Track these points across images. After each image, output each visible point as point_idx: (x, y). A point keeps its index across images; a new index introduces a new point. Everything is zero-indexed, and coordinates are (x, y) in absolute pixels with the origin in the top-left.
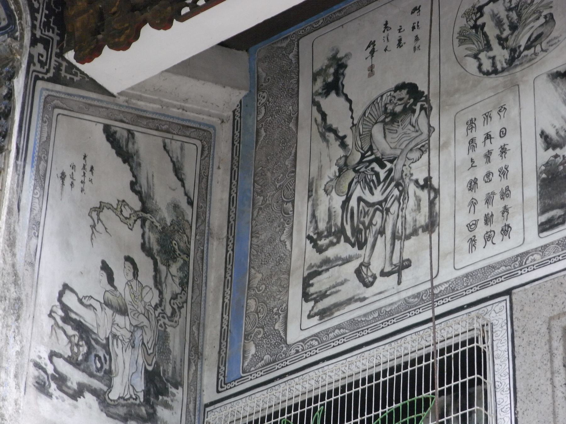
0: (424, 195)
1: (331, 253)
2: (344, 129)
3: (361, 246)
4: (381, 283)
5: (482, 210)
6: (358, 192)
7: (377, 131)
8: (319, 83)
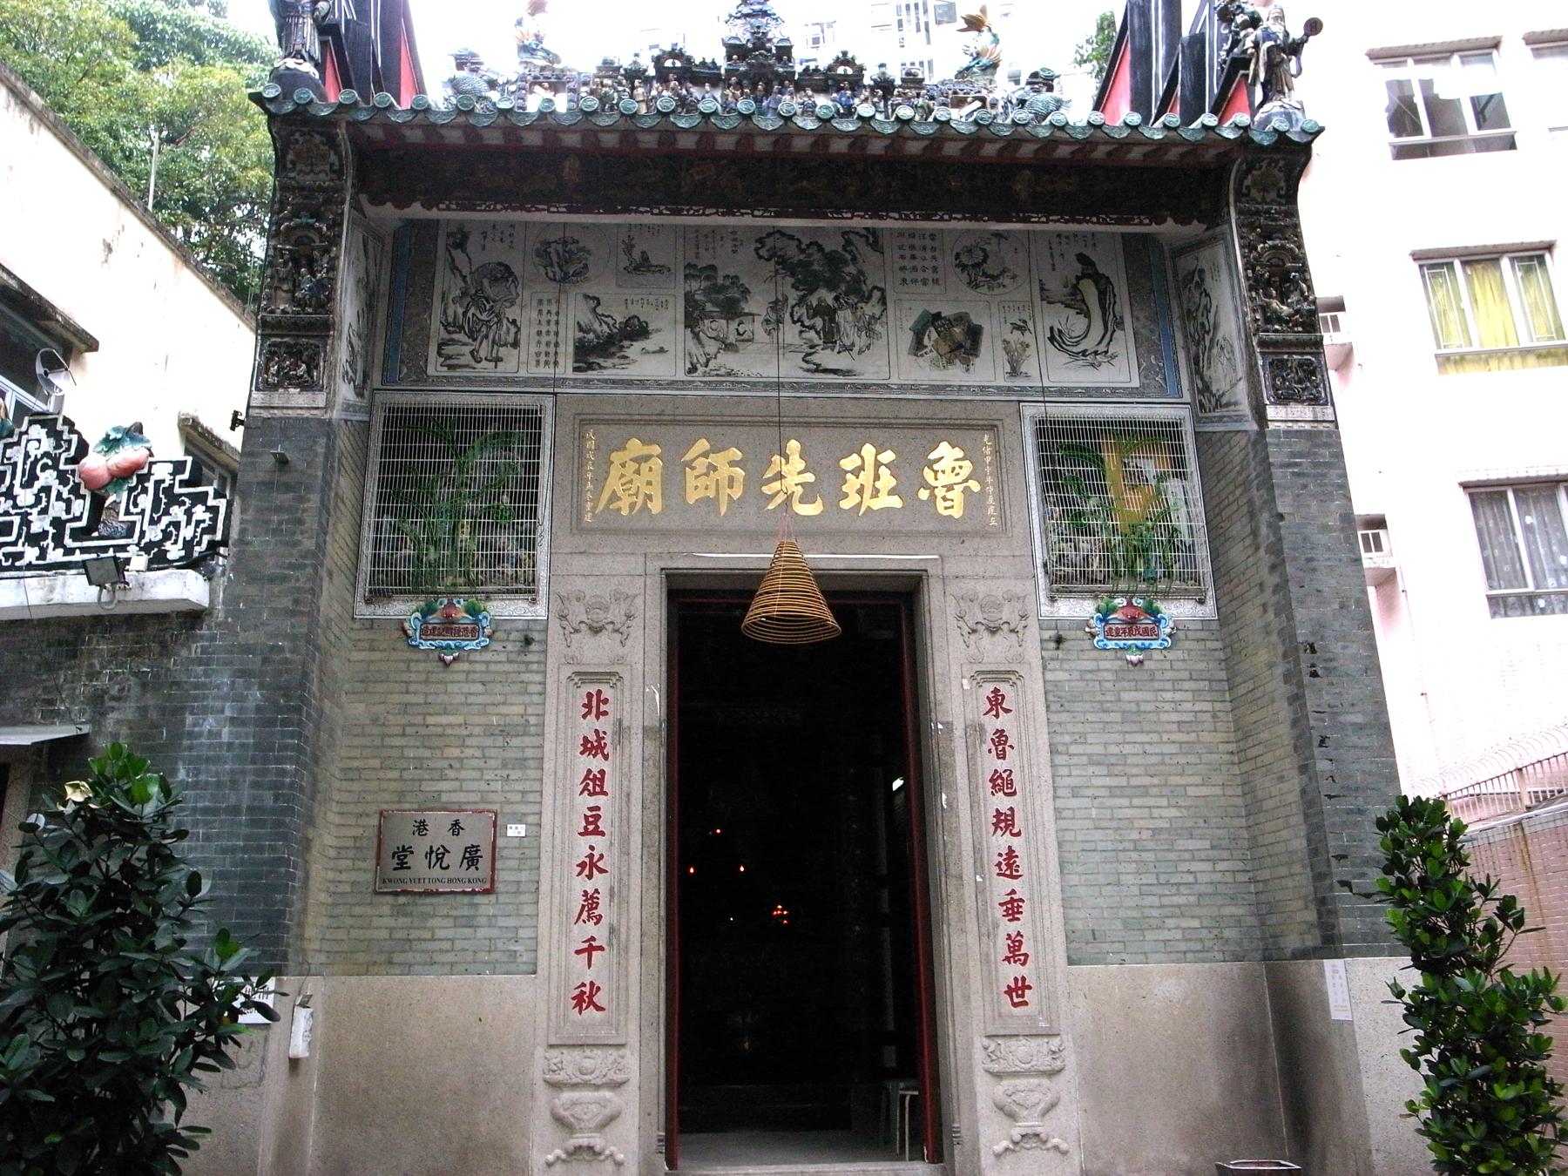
0: (513, 330)
1: (455, 336)
2: (466, 272)
3: (474, 340)
4: (484, 364)
5: (543, 348)
6: (472, 310)
7: (486, 282)
8: (451, 240)
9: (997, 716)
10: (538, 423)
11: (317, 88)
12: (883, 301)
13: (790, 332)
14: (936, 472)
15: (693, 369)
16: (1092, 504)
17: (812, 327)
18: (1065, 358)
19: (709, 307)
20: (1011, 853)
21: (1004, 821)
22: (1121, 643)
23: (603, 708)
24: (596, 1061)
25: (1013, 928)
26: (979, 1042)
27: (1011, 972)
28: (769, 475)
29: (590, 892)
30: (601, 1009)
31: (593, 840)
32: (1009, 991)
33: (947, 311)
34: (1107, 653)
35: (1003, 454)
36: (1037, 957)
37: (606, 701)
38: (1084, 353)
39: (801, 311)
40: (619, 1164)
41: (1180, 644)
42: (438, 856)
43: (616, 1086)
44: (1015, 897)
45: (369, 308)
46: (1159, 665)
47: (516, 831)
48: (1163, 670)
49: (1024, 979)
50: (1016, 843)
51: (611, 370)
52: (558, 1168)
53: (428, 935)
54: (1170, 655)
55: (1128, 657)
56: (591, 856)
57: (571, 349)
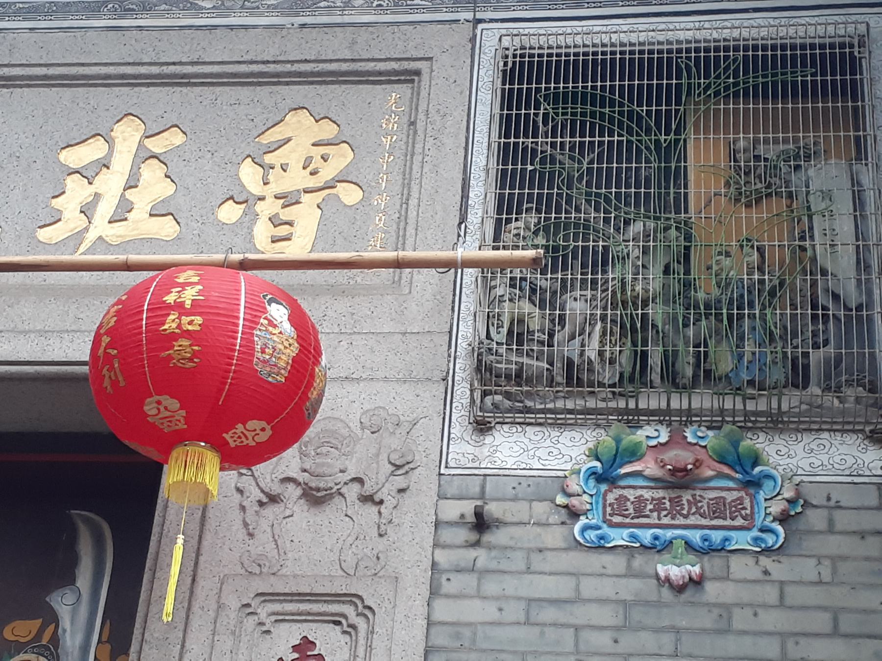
22: (646, 536)
34: (607, 559)
35: (420, 125)
41: (812, 544)
46: (745, 594)
48: (756, 608)
54: (779, 569)
55: (661, 570)
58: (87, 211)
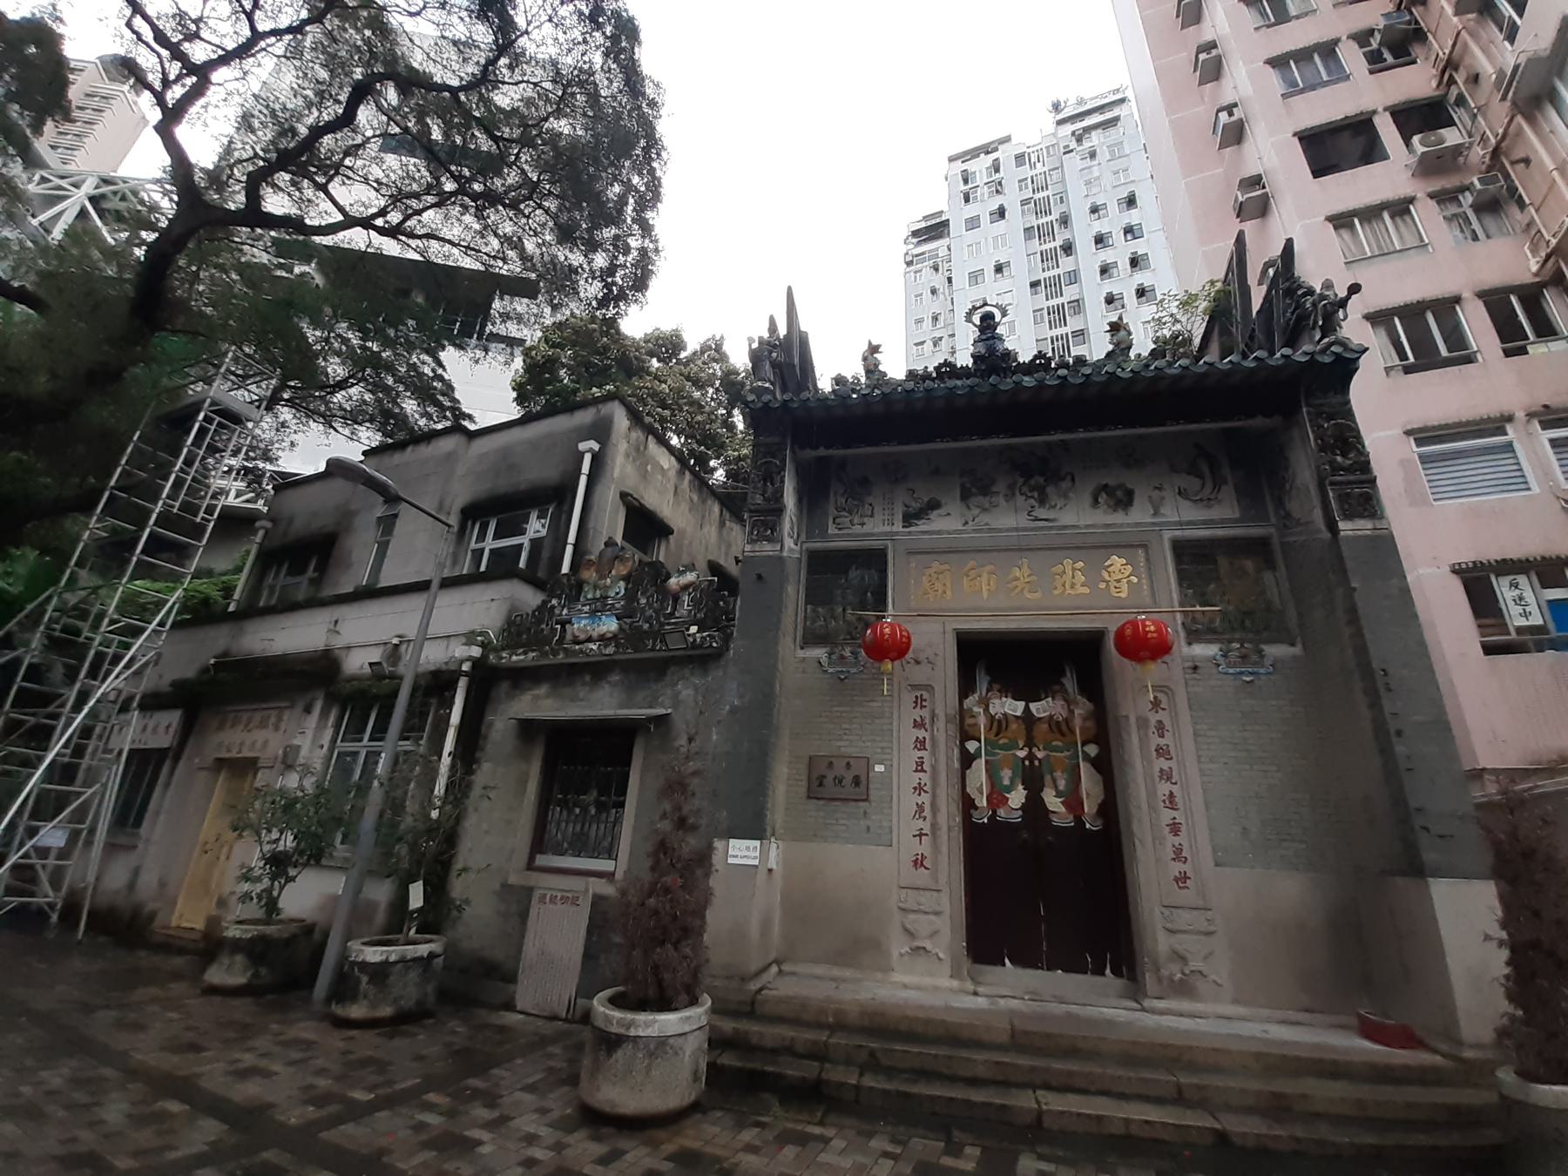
1: (842, 513)
9: (1157, 712)
10: (885, 556)
11: (774, 394)
12: (1073, 480)
13: (1020, 499)
14: (1109, 572)
15: (967, 523)
16: (1212, 586)
17: (1032, 497)
18: (1188, 503)
19: (974, 490)
20: (1171, 793)
21: (1166, 776)
22: (1238, 670)
23: (924, 703)
24: (926, 900)
25: (1176, 840)
26: (1157, 911)
27: (1177, 868)
28: (1011, 576)
29: (920, 803)
30: (926, 868)
31: (921, 775)
32: (1176, 880)
33: (1112, 482)
36: (1192, 860)
37: (925, 700)
38: (1201, 500)
39: (1025, 489)
40: (940, 959)
42: (839, 781)
43: (937, 913)
44: (1177, 821)
45: (800, 501)
47: (879, 768)
49: (1185, 873)
50: (1175, 789)
51: (922, 526)
52: (906, 958)
53: (834, 822)
54: (1272, 677)
56: (920, 784)
57: (901, 517)
58: (1064, 586)
